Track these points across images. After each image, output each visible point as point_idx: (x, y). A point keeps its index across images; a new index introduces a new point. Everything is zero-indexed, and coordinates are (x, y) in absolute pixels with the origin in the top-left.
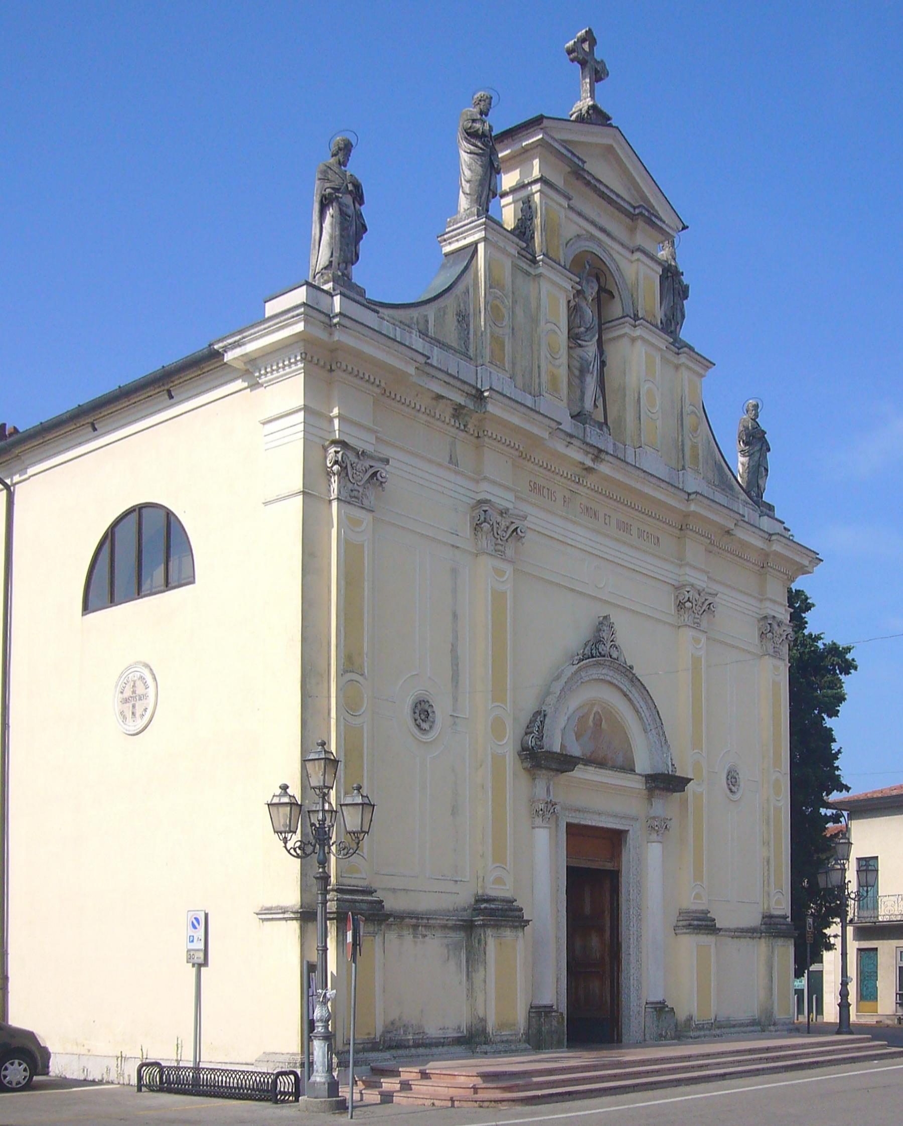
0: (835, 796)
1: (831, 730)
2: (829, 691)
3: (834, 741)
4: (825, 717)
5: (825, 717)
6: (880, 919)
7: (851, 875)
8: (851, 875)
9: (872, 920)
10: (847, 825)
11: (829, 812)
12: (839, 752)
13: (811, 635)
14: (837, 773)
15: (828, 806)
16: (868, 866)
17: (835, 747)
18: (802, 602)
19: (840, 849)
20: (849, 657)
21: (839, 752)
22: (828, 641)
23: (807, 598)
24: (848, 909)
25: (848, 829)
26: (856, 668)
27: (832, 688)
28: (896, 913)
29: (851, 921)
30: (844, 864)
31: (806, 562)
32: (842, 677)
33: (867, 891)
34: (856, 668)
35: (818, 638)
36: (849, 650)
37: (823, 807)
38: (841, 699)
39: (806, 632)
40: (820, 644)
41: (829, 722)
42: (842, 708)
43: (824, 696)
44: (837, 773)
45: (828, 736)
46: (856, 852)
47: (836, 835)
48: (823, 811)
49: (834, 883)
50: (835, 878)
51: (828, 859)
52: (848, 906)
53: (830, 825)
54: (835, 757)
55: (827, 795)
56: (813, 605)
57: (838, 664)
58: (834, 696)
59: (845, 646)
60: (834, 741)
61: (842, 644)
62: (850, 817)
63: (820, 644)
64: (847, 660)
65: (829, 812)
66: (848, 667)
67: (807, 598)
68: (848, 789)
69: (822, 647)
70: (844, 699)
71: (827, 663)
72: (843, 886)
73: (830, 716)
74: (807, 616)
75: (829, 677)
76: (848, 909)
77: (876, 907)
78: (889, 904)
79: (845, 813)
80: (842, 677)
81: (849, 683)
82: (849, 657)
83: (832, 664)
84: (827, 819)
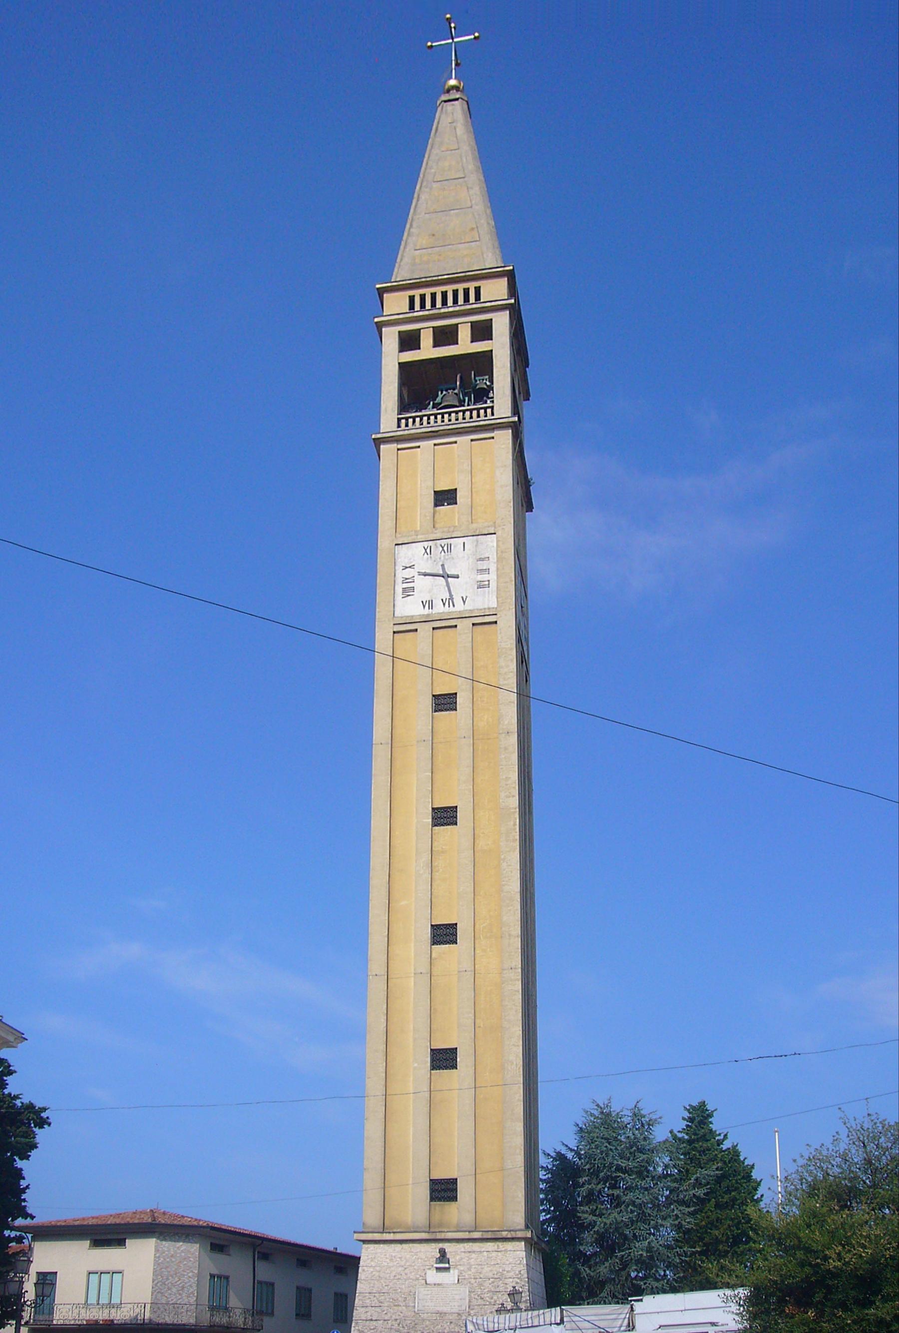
0: (20, 1222)
1: (21, 1170)
2: (23, 1140)
3: (24, 1178)
4: (17, 1158)
5: (17, 1158)
6: (55, 1322)
7: (30, 1291)
8: (30, 1291)
9: (47, 1323)
10: (30, 1245)
11: (13, 1234)
12: (27, 1187)
13: (10, 1094)
14: (23, 1204)
15: (12, 1229)
16: (47, 1281)
17: (23, 1183)
18: (5, 1068)
19: (20, 1265)
20: (44, 1115)
21: (27, 1187)
22: (26, 1101)
23: (10, 1066)
24: (23, 1314)
25: (30, 1248)
26: (49, 1124)
27: (26, 1137)
28: (70, 1318)
29: (27, 1323)
30: (22, 1277)
31: (11, 1038)
32: (36, 1130)
33: (43, 1300)
34: (49, 1124)
35: (16, 1097)
36: (44, 1109)
37: (7, 1229)
38: (34, 1146)
39: (6, 1091)
40: (18, 1103)
41: (20, 1163)
42: (33, 1153)
43: (17, 1142)
44: (23, 1204)
45: (18, 1174)
46: (34, 1269)
47: (17, 1253)
48: (7, 1233)
49: (11, 1292)
50: (13, 1288)
51: (8, 1272)
52: (23, 1311)
53: (14, 1244)
54: (23, 1191)
55: (12, 1220)
56: (15, 1072)
57: (33, 1119)
58: (26, 1144)
59: (41, 1106)
60: (24, 1178)
61: (38, 1104)
62: (34, 1239)
63: (18, 1103)
64: (42, 1117)
65: (13, 1234)
66: (43, 1123)
67: (10, 1066)
68: (33, 1217)
69: (20, 1105)
70: (37, 1147)
71: (24, 1117)
72: (20, 1294)
73: (21, 1159)
74: (9, 1079)
75: (24, 1128)
76: (23, 1314)
77: (51, 1312)
78: (64, 1311)
79: (30, 1236)
80: (36, 1130)
81: (41, 1135)
82: (44, 1115)
83: (28, 1119)
84: (10, 1240)
